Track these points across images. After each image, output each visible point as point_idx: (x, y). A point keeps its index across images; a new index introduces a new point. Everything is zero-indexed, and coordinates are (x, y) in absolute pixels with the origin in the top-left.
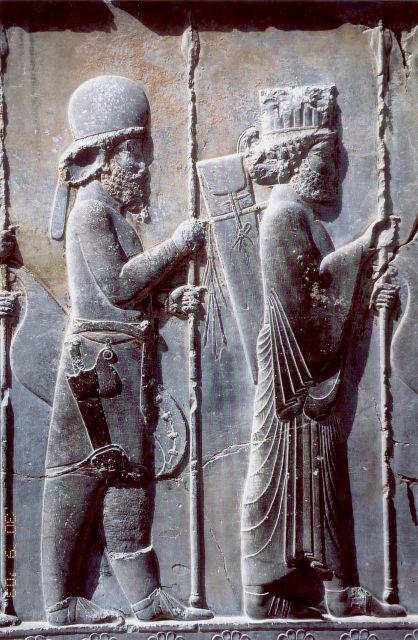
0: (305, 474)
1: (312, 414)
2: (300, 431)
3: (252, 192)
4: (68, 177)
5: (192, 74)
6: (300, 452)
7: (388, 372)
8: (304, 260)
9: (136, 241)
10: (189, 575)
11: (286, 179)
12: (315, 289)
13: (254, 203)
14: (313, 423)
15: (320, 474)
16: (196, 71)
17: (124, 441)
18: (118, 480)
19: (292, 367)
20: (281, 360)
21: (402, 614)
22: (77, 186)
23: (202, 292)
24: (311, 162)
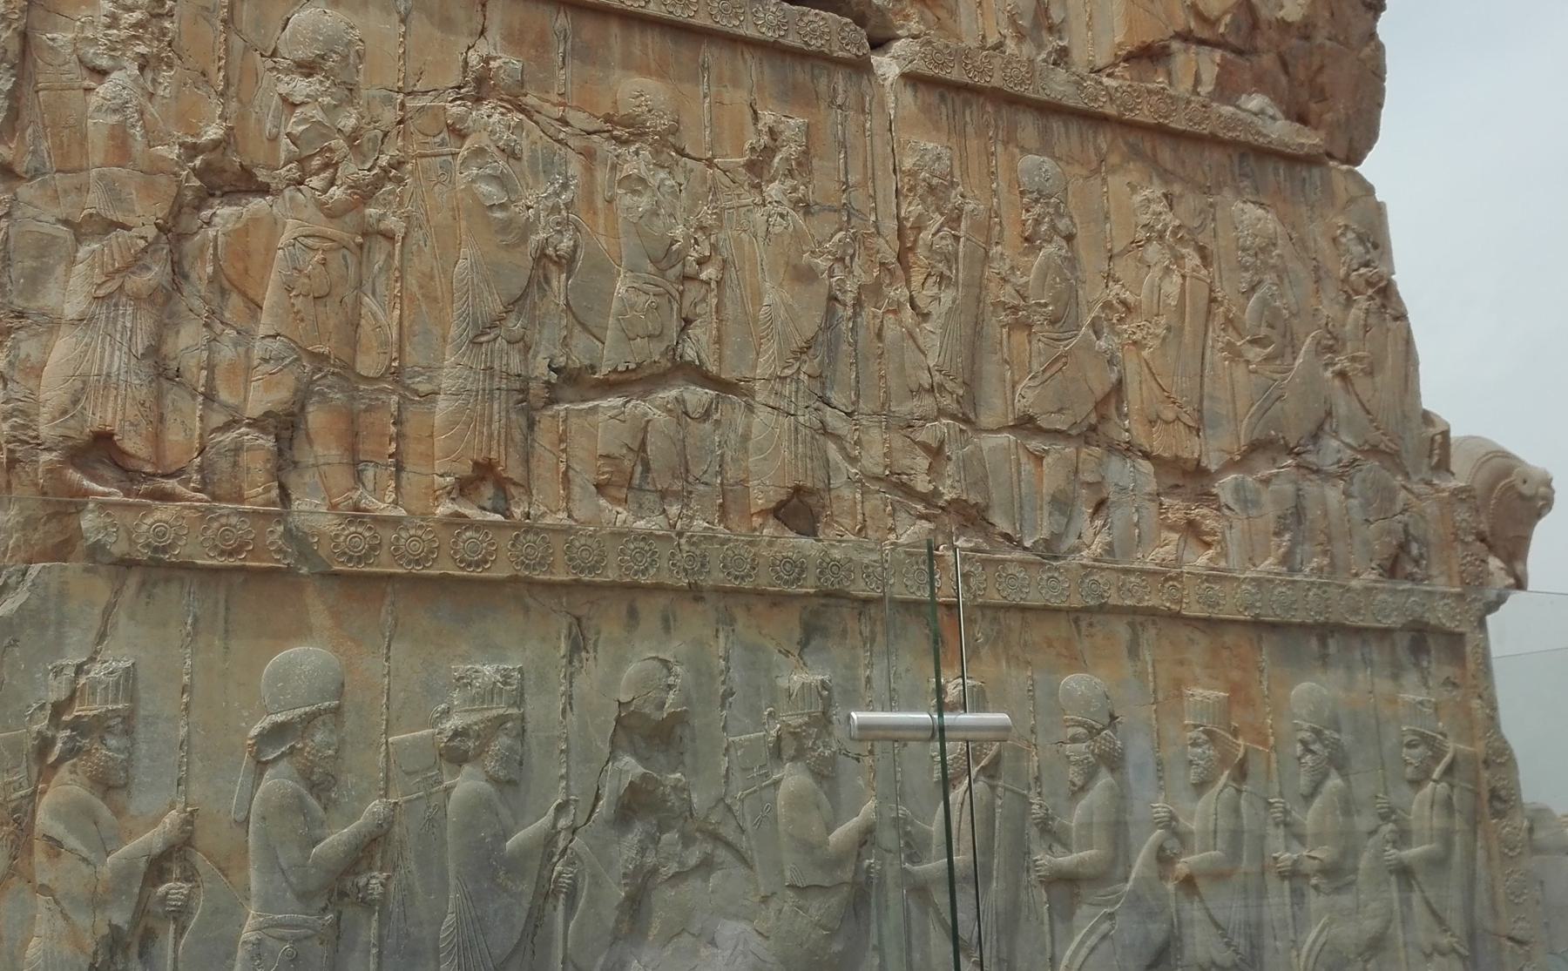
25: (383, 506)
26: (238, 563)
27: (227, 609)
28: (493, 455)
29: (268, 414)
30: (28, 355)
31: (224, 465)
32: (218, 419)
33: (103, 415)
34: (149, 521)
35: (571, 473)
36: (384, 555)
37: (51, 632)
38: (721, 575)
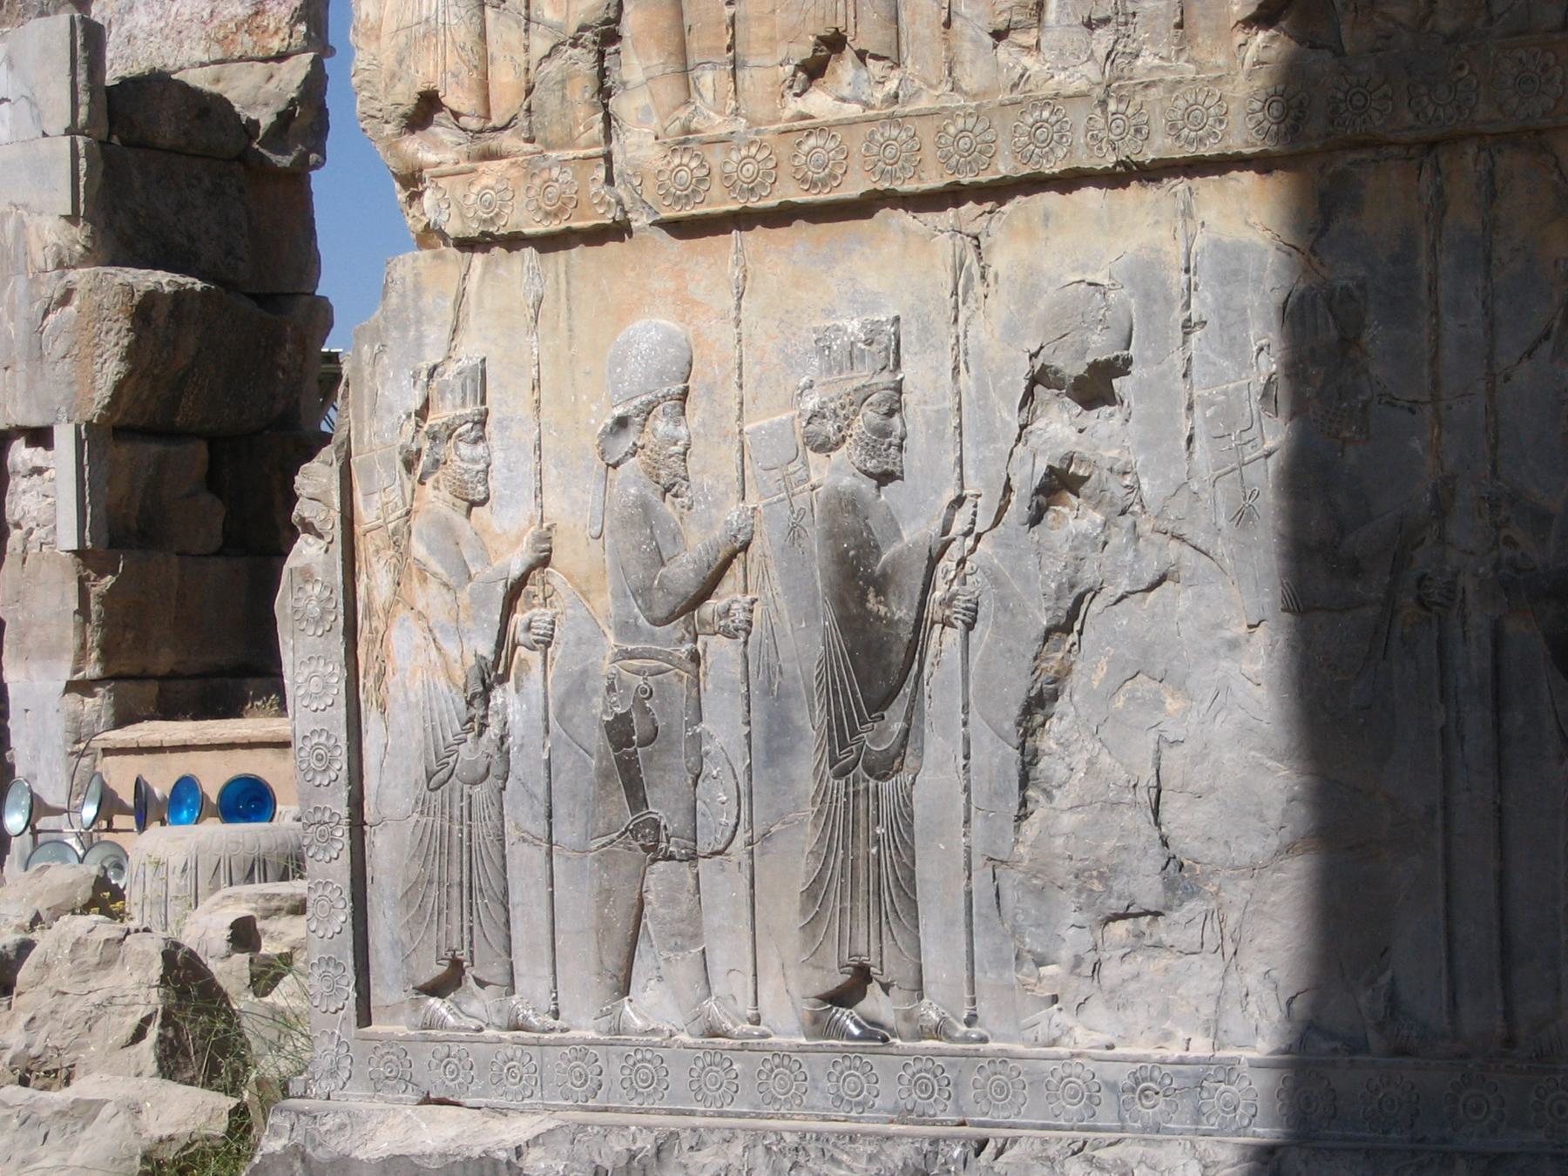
0: (862, 852)
1: (870, 771)
2: (856, 794)
3: (805, 464)
4: (603, 454)
5: (739, 307)
6: (855, 822)
7: (966, 708)
8: (856, 557)
9: (676, 536)
10: (746, 983)
11: (837, 445)
12: (871, 596)
13: (808, 478)
14: (872, 783)
15: (879, 852)
16: (743, 303)
17: (663, 806)
18: (654, 852)
19: (847, 705)
20: (833, 692)
21: (984, 1040)
22: (615, 466)
23: (753, 602)
24: (868, 416)
25: (715, 123)
26: (563, 226)
27: (568, 283)
28: (840, 24)
29: (583, 28)
30: (368, 15)
31: (553, 102)
32: (540, 46)
33: (424, 73)
34: (475, 189)
35: (957, 24)
36: (717, 190)
37: (412, 333)
38: (1169, 141)
